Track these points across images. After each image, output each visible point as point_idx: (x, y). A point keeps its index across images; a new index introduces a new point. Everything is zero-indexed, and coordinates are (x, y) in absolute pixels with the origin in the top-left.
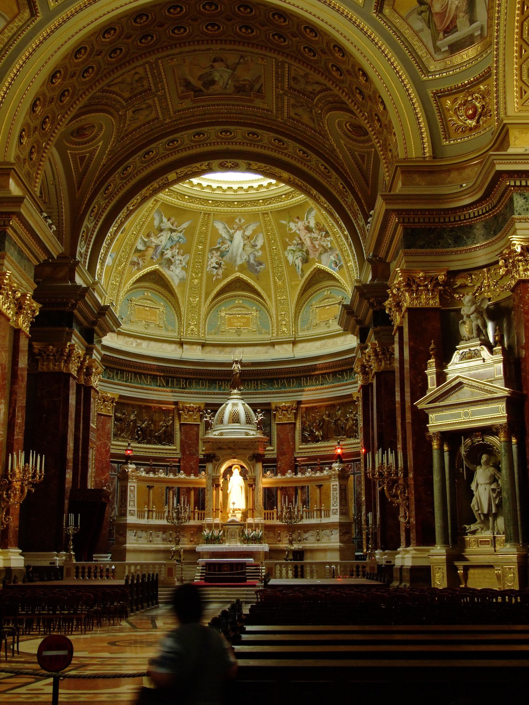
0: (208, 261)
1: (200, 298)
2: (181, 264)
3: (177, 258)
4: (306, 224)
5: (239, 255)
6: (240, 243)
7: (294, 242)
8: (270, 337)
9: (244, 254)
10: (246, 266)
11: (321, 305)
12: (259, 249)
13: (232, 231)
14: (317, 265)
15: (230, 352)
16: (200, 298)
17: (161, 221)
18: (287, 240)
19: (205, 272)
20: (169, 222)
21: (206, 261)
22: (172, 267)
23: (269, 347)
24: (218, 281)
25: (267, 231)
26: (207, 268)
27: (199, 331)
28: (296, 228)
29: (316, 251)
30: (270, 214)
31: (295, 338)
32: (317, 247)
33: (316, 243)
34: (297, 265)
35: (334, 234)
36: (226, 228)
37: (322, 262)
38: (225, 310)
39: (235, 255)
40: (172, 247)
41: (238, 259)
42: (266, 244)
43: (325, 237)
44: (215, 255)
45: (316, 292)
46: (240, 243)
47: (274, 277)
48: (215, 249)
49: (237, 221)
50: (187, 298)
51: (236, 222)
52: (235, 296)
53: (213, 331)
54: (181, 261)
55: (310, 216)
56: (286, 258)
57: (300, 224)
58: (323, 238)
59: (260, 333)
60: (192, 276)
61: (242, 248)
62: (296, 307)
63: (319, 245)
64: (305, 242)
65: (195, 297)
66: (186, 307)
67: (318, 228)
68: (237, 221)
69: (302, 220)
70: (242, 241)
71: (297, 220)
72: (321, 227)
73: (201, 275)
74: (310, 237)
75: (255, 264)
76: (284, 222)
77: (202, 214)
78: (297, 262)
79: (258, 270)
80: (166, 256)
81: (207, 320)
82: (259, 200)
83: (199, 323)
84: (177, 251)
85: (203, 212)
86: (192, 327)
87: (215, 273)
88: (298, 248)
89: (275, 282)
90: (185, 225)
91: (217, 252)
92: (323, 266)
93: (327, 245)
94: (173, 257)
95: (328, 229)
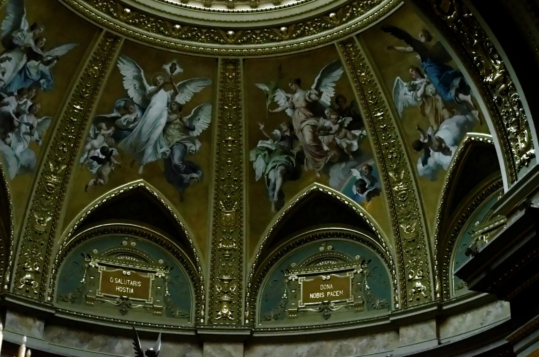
0: (86, 143)
1: (55, 217)
2: (31, 134)
3: (25, 118)
4: (313, 97)
5: (152, 142)
6: (160, 116)
7: (277, 132)
8: (190, 324)
9: (163, 143)
10: (162, 168)
11: (309, 273)
12: (198, 137)
13: (150, 88)
14: (315, 186)
15: (104, 346)
16: (55, 217)
17: (16, 26)
18: (262, 127)
19: (75, 163)
20: (31, 34)
21: (82, 141)
22: (12, 137)
23: (189, 346)
24: (99, 189)
25: (224, 100)
26: (82, 155)
27: (42, 289)
28: (287, 104)
29: (321, 157)
30: (241, 66)
31: (252, 332)
32: (326, 148)
33: (325, 140)
34: (273, 181)
35: (374, 122)
36: (138, 78)
37: (331, 181)
38: (99, 256)
39: (144, 139)
40: (21, 93)
41: (149, 150)
42: (216, 131)
43: (350, 127)
44: (103, 132)
45: (299, 244)
46: (160, 116)
47: (217, 199)
48: (105, 120)
49: (167, 67)
50: (28, 212)
51: (165, 70)
52: (122, 231)
53: (70, 296)
54: (32, 127)
55: (326, 81)
56: (251, 163)
57: (299, 97)
58: (344, 130)
59: (170, 314)
60: (47, 165)
61: (160, 129)
62: (256, 268)
63: (329, 145)
64: (299, 136)
65: (44, 214)
66: (24, 230)
67: (337, 107)
68: (167, 67)
69: (306, 87)
70: (165, 114)
71: (293, 87)
72: (345, 106)
73: (66, 169)
74: (314, 127)
75: (183, 167)
76: (264, 87)
77: (103, 33)
78: (272, 176)
79: (186, 181)
80: (6, 109)
81: (60, 270)
82: (227, 29)
83: (45, 270)
84: (30, 103)
85: (105, 29)
86: (28, 276)
87: (94, 171)
88: (281, 147)
89: (218, 212)
90: (60, 51)
91: (108, 128)
92: (331, 190)
93: (350, 146)
94: (18, 114)
95: (363, 112)
